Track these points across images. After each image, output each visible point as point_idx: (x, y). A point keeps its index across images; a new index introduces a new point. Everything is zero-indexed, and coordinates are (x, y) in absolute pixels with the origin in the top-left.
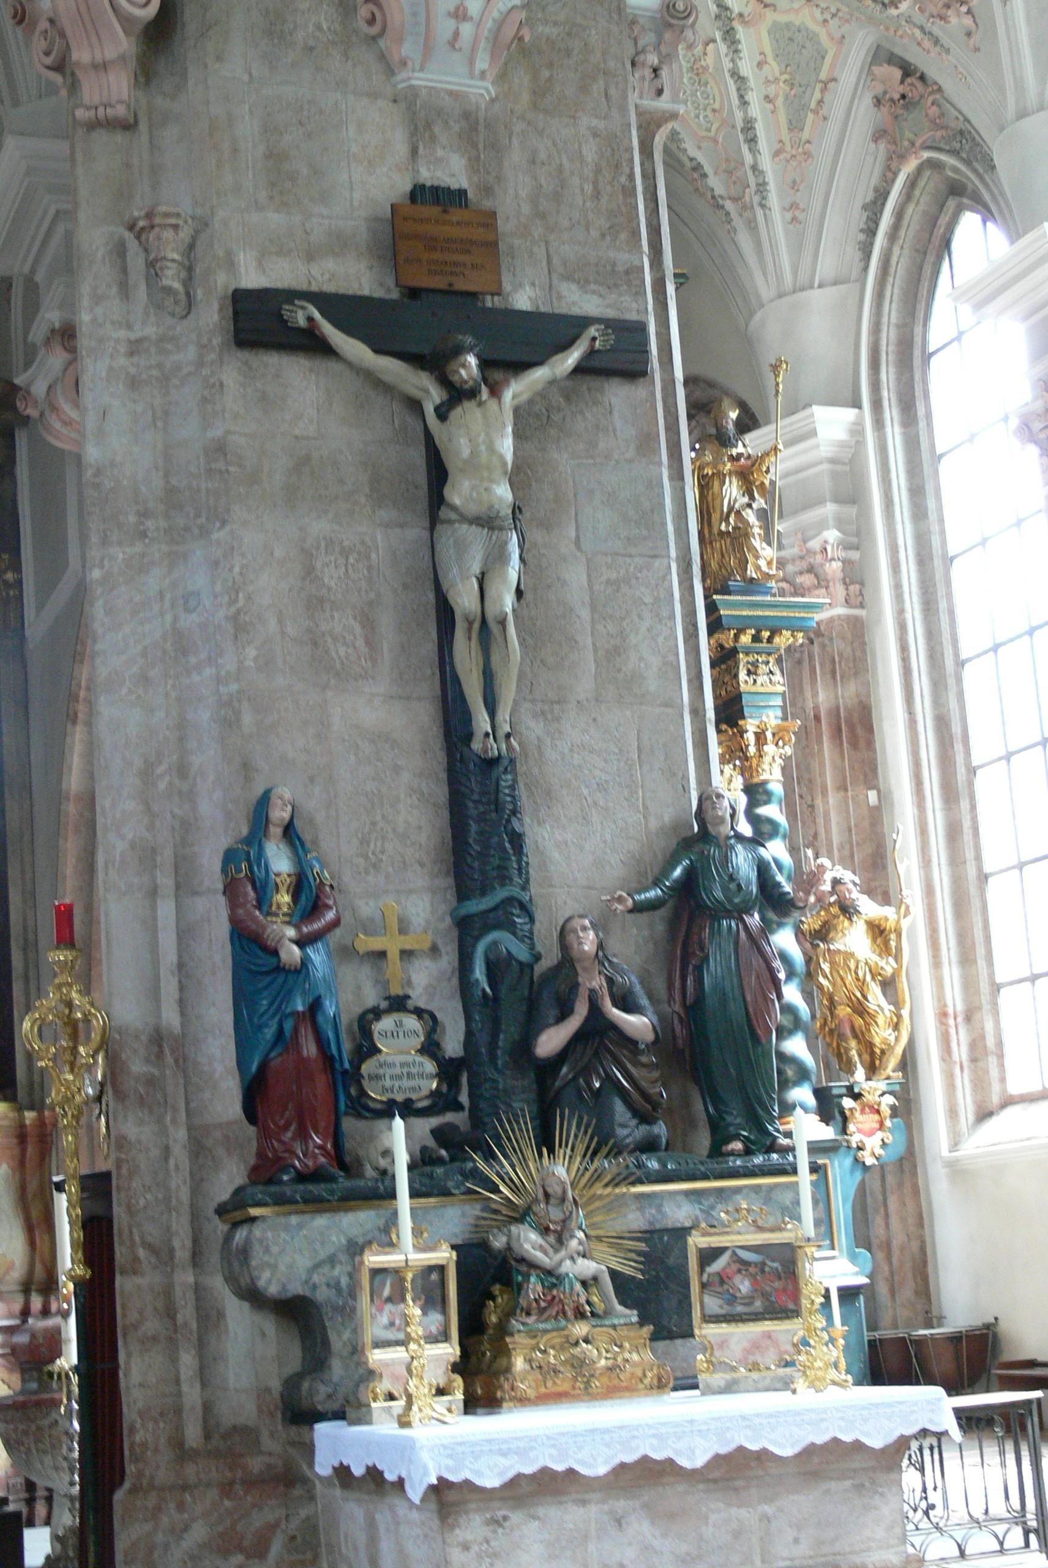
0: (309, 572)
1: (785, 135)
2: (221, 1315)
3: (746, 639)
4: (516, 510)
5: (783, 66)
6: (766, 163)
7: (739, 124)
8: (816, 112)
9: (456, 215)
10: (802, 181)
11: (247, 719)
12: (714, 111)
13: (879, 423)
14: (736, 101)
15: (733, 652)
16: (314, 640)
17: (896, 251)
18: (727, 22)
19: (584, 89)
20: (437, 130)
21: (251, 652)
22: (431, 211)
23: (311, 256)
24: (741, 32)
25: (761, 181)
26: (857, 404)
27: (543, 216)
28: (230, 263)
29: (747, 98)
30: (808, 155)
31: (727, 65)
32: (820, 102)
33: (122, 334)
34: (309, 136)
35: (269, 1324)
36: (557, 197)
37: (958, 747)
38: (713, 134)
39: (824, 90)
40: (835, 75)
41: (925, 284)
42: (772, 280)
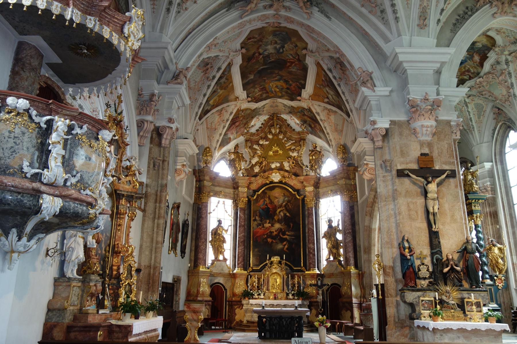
0: (408, 206)
1: (477, 120)
2: (400, 304)
3: (473, 201)
4: (438, 197)
6: (474, 124)
7: (469, 118)
9: (427, 157)
11: (401, 226)
13: (496, 165)
14: (468, 115)
15: (471, 203)
16: (409, 215)
17: (498, 137)
19: (445, 137)
20: (424, 145)
21: (401, 217)
22: (423, 157)
23: (407, 164)
24: (469, 105)
26: (492, 162)
27: (439, 155)
28: (396, 166)
30: (481, 122)
31: (466, 110)
32: (483, 114)
33: (382, 175)
34: (406, 148)
35: (407, 306)
36: (441, 153)
37: (514, 219)
41: (504, 142)
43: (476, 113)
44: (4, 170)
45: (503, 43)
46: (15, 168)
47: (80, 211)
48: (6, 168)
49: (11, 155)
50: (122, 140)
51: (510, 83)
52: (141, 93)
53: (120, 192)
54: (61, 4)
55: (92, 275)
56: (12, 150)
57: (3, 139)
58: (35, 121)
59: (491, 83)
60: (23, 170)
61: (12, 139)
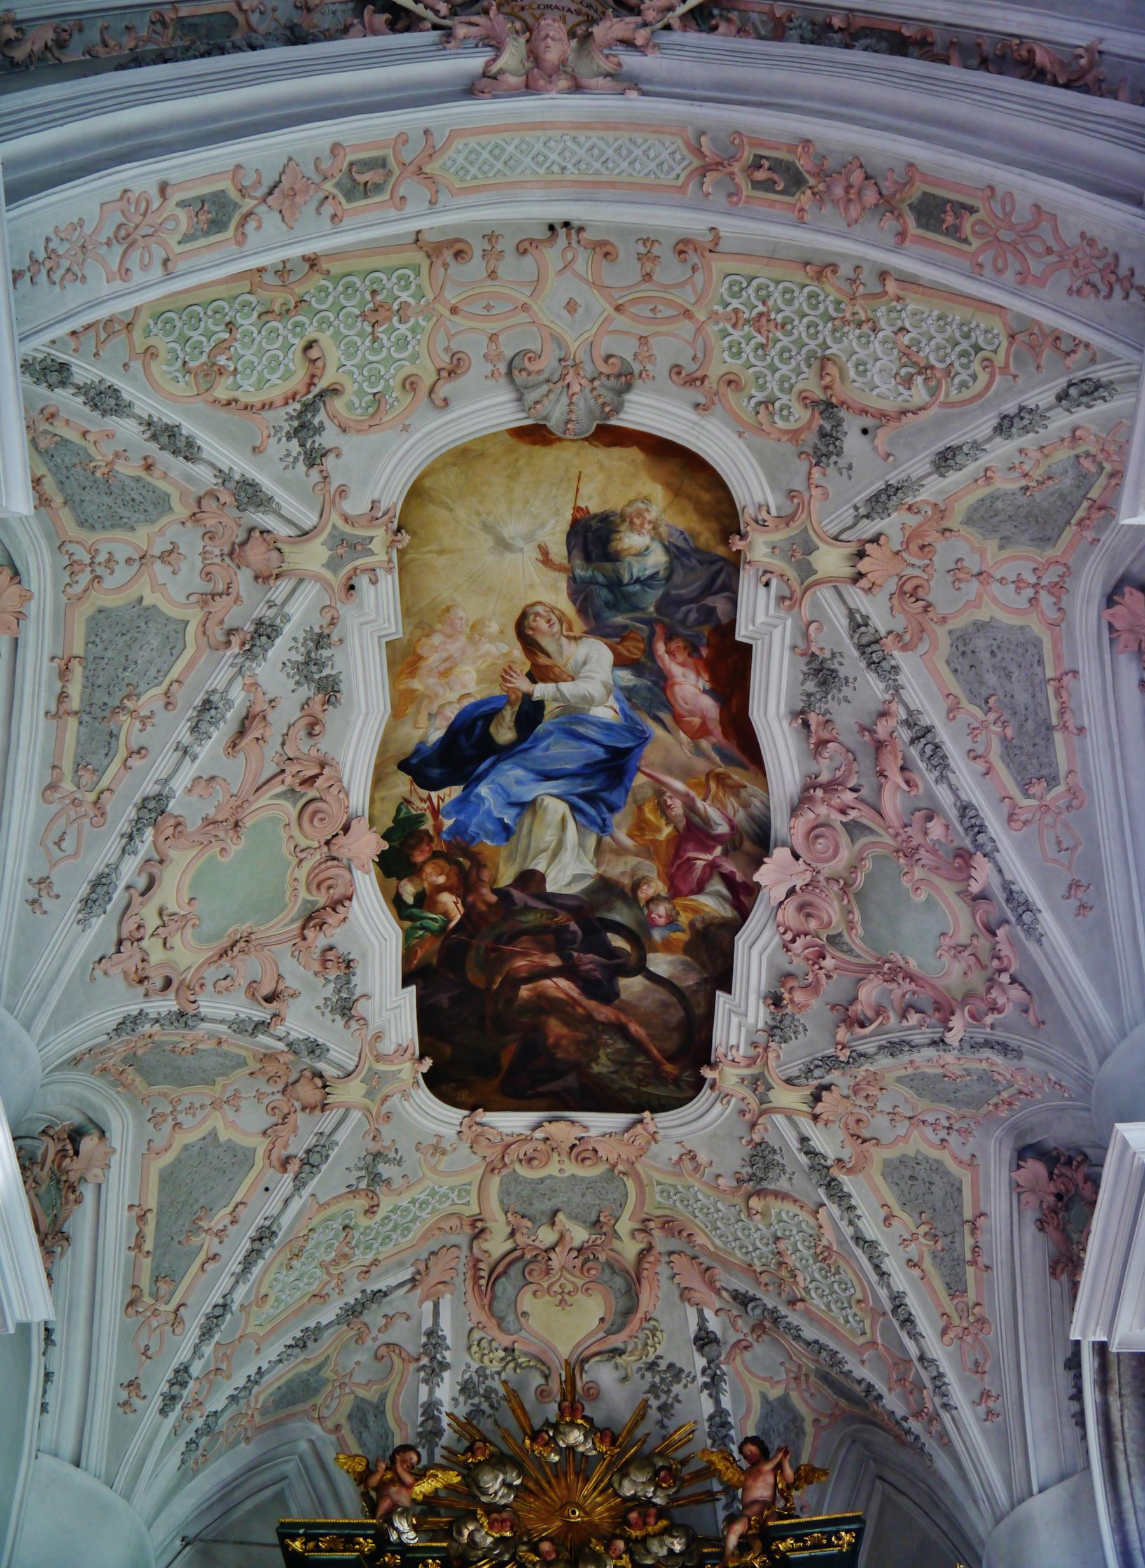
1: (949, 1306)
5: (916, 1215)
6: (935, 1348)
7: (888, 1306)
8: (974, 1263)
10: (986, 1360)
12: (859, 1301)
14: (874, 1278)
17: (1115, 1404)
18: (824, 1171)
24: (848, 1183)
25: (935, 1374)
29: (884, 1267)
30: (981, 1321)
31: (849, 1231)
32: (975, 1249)
38: (868, 1337)
39: (974, 1230)
40: (983, 1209)
42: (984, 1506)
43: (920, 1248)
45: (774, 487)
51: (953, 814)
59: (860, 879)
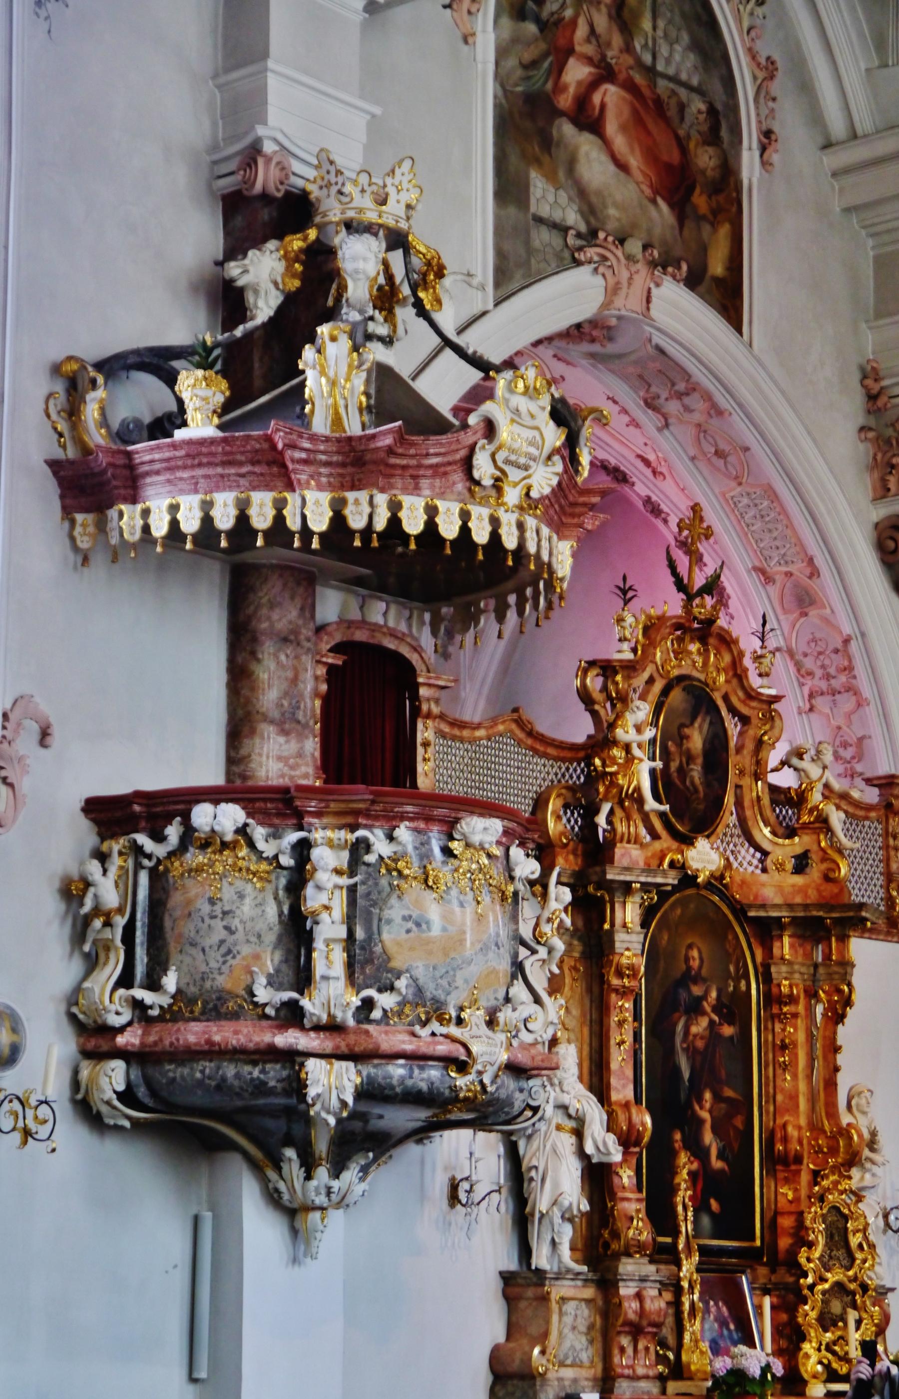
44: (215, 1007)
46: (237, 996)
47: (424, 1086)
48: (219, 999)
49: (224, 963)
50: (743, 688)
52: (875, 388)
53: (762, 914)
54: (271, 490)
55: (624, 1260)
56: (223, 950)
57: (200, 924)
58: (264, 855)
60: (255, 999)
61: (218, 920)
